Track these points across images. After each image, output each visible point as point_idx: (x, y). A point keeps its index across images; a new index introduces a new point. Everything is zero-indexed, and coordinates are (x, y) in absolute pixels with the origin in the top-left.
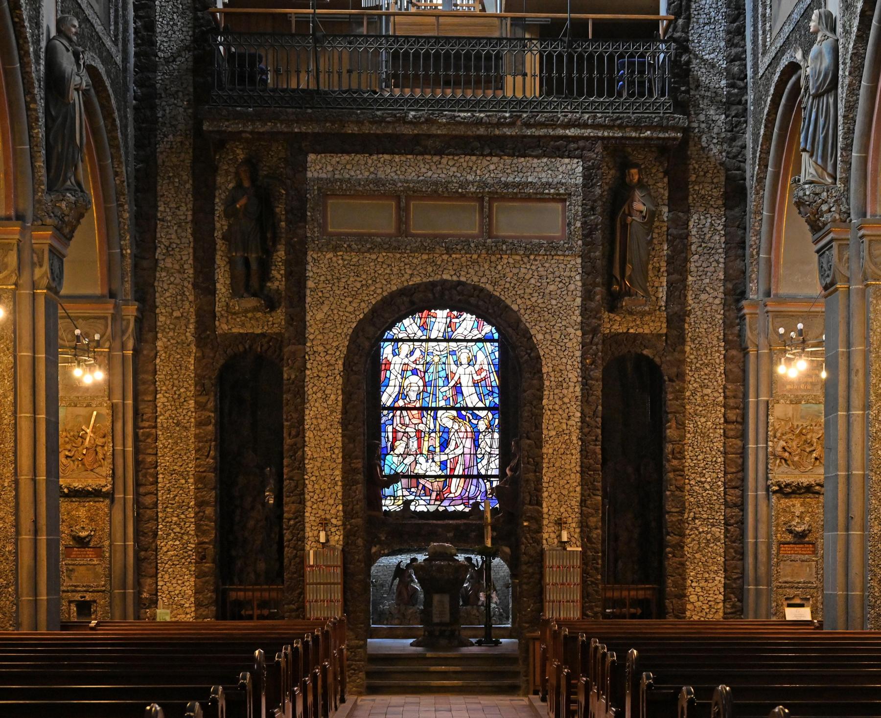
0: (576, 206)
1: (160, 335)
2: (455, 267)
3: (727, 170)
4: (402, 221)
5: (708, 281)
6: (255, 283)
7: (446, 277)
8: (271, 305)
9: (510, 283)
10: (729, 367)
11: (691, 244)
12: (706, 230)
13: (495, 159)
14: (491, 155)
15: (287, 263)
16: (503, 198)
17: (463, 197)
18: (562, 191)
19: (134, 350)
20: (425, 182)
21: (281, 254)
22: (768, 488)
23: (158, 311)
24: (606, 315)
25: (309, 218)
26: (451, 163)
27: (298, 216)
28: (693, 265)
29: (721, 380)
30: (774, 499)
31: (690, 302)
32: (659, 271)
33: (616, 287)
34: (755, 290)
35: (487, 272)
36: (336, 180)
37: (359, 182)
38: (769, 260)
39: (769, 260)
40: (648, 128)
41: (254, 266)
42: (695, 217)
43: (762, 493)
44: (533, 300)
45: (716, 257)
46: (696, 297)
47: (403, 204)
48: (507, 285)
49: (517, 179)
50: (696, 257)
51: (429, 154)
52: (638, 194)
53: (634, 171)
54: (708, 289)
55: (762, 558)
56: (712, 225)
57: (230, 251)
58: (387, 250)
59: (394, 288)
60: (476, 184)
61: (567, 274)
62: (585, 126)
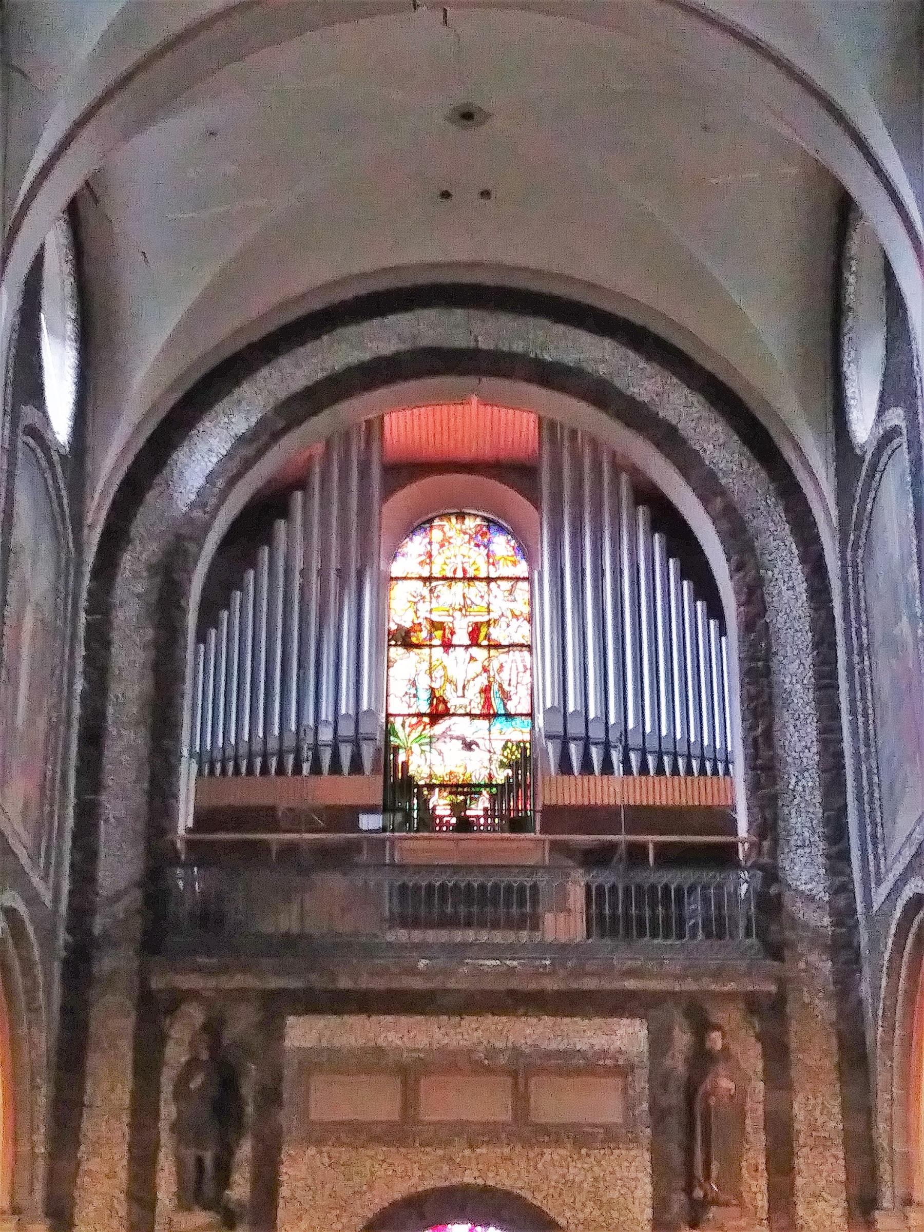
0: (641, 1083)
2: (480, 1167)
4: (409, 1102)
5: (823, 1183)
6: (209, 1188)
12: (817, 1113)
13: (534, 1020)
14: (525, 1015)
16: (542, 1070)
17: (490, 1070)
18: (621, 1062)
21: (245, 1150)
26: (474, 1026)
28: (801, 1160)
31: (801, 1213)
32: (757, 1170)
33: (698, 1193)
45: (833, 1151)
48: (552, 1191)
50: (806, 1150)
53: (716, 1035)
62: (652, 976)
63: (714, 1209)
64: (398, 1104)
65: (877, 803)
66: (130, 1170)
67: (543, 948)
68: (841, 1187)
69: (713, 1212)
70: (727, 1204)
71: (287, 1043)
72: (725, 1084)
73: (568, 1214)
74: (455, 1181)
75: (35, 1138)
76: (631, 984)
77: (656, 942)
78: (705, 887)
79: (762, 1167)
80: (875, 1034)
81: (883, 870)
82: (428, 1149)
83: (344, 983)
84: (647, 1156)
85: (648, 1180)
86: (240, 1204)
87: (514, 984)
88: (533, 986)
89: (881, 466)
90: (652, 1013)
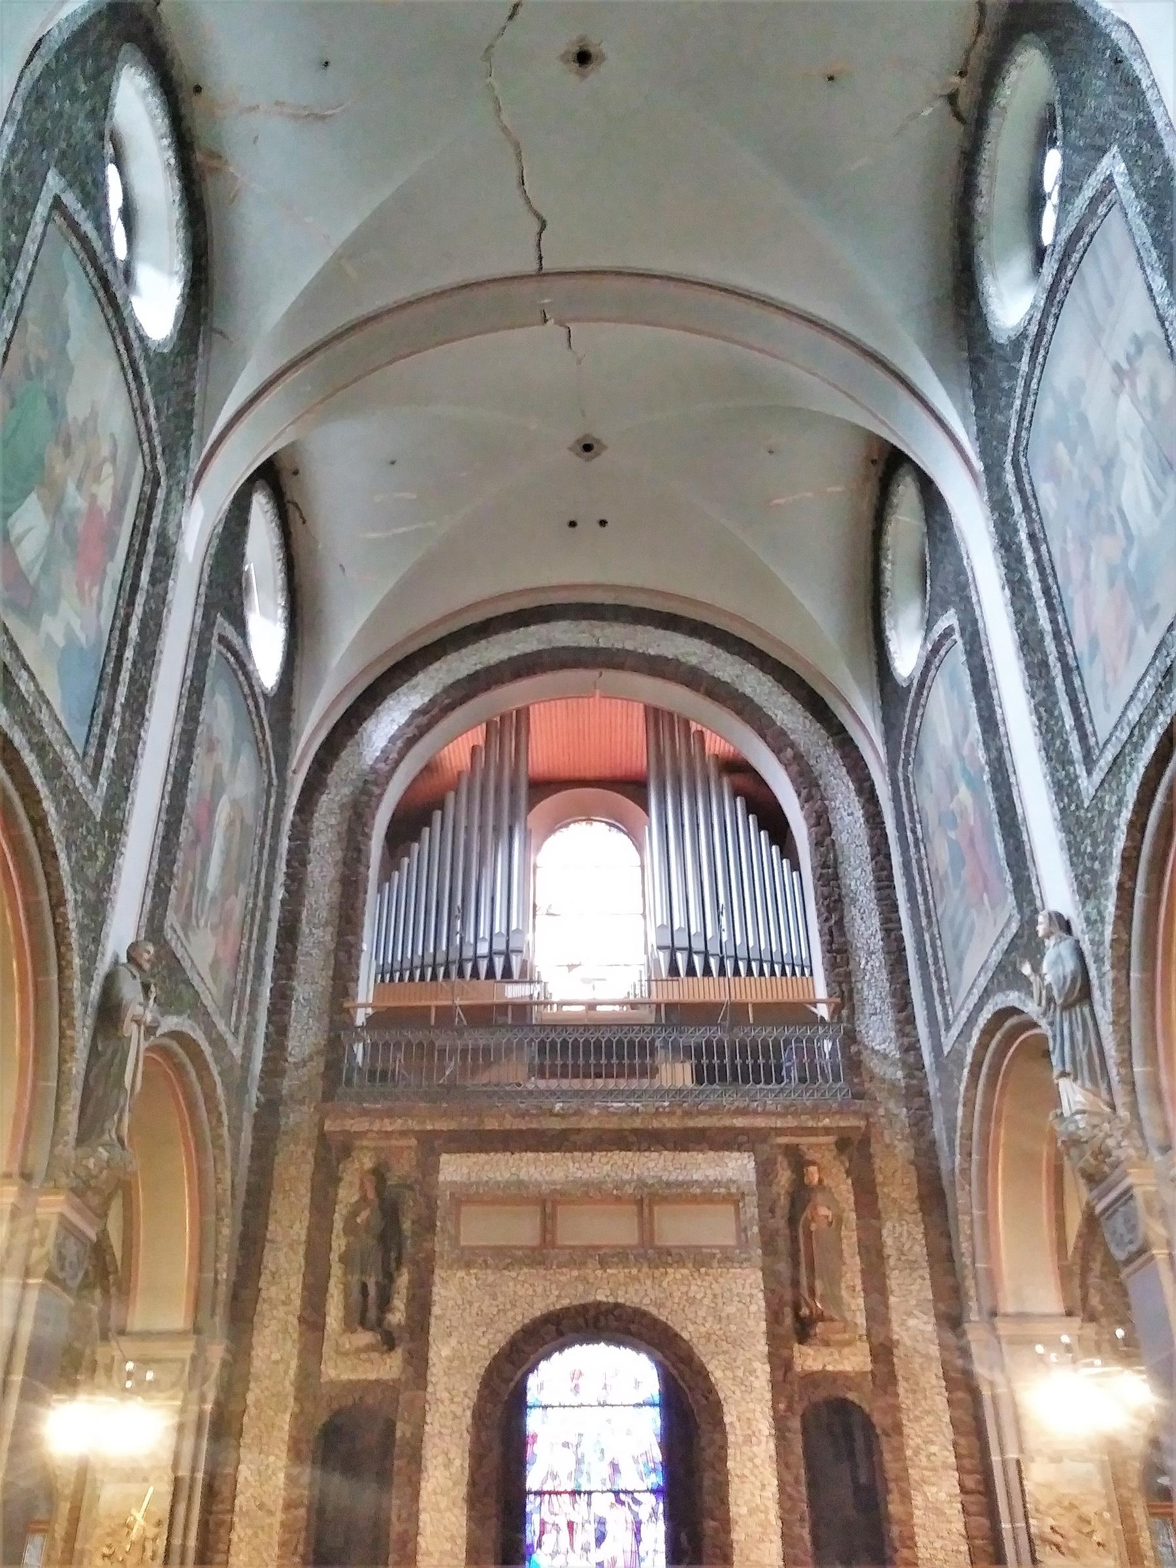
0: (751, 1210)
1: (252, 1385)
6: (372, 1314)
7: (601, 1297)
8: (389, 1342)
9: (679, 1304)
11: (889, 1256)
12: (904, 1239)
13: (655, 1155)
14: (648, 1149)
15: (412, 1283)
16: (665, 1199)
17: (618, 1199)
18: (733, 1190)
19: (217, 1403)
20: (575, 1182)
21: (403, 1280)
23: (253, 1353)
24: (796, 1346)
25: (438, 1229)
27: (427, 1226)
33: (805, 1311)
35: (650, 1292)
36: (471, 1184)
37: (498, 1183)
40: (829, 1113)
41: (372, 1291)
42: (889, 1225)
44: (707, 1325)
45: (921, 1272)
46: (903, 1323)
47: (548, 1210)
49: (681, 1178)
50: (897, 1272)
51: (579, 1150)
52: (819, 1197)
54: (916, 1312)
56: (909, 1233)
57: (345, 1274)
58: (530, 1265)
59: (538, 1314)
60: (633, 1185)
61: (747, 1291)
62: (755, 1113)
63: (820, 1324)
64: (538, 1232)
65: (941, 963)
66: (303, 1299)
67: (662, 1093)
68: (930, 1306)
69: (820, 1328)
70: (832, 1320)
71: (441, 1178)
72: (823, 1211)
73: (691, 1328)
74: (590, 1299)
75: (218, 1265)
76: (739, 1122)
77: (758, 1086)
78: (799, 1041)
79: (859, 1288)
80: (951, 1161)
81: (951, 1017)
82: (564, 1270)
83: (491, 1124)
84: (760, 1274)
85: (761, 1295)
86: (399, 1325)
87: (637, 1123)
88: (655, 1124)
90: (758, 1146)
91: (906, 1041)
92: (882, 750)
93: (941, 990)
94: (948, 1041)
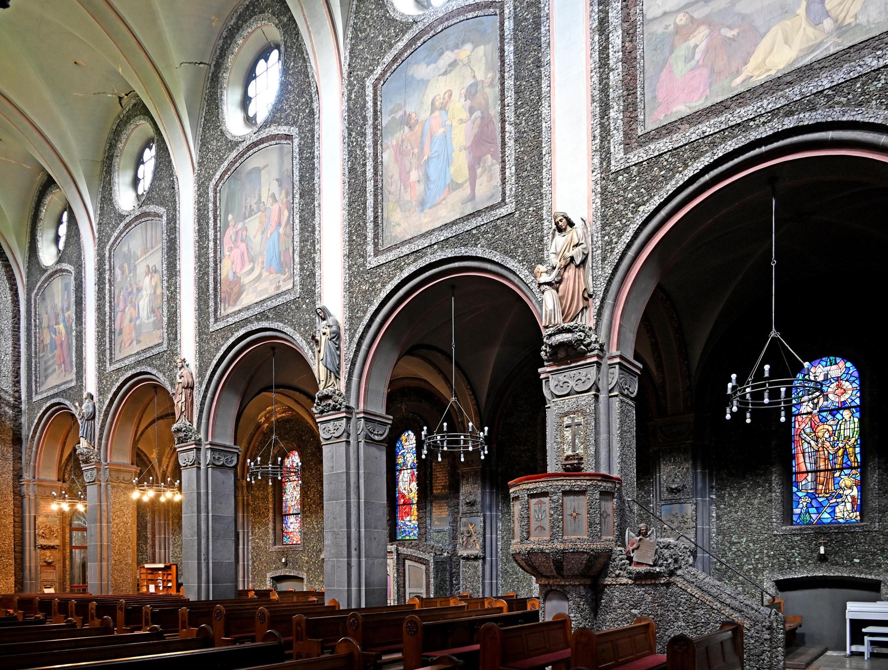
3: (14, 431)
10: (16, 502)
22: (35, 546)
29: (12, 507)
30: (38, 551)
34: (27, 476)
38: (35, 466)
39: (35, 466)
43: (32, 548)
55: (33, 571)
89: (55, 276)
91: (16, 389)
92: (25, 280)
93: (36, 381)
94: (35, 398)
